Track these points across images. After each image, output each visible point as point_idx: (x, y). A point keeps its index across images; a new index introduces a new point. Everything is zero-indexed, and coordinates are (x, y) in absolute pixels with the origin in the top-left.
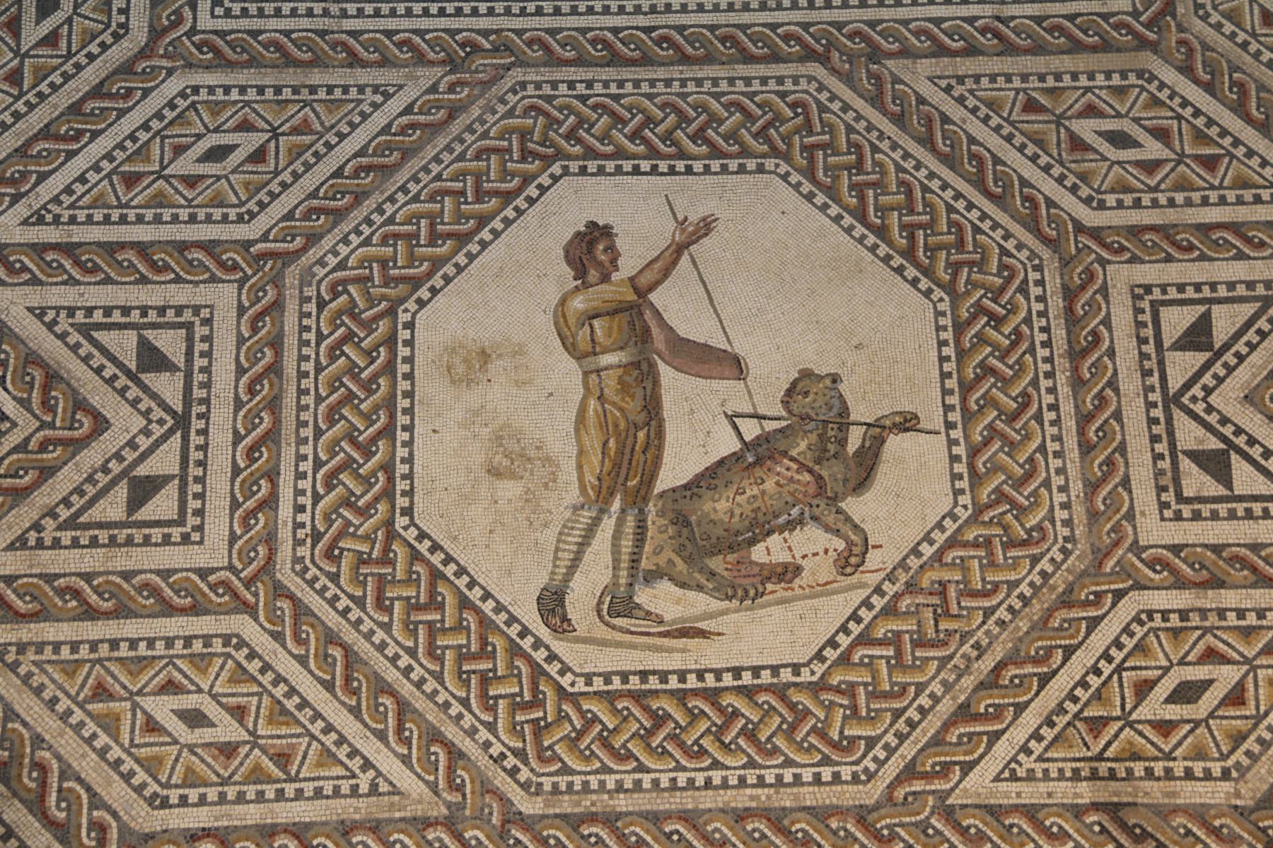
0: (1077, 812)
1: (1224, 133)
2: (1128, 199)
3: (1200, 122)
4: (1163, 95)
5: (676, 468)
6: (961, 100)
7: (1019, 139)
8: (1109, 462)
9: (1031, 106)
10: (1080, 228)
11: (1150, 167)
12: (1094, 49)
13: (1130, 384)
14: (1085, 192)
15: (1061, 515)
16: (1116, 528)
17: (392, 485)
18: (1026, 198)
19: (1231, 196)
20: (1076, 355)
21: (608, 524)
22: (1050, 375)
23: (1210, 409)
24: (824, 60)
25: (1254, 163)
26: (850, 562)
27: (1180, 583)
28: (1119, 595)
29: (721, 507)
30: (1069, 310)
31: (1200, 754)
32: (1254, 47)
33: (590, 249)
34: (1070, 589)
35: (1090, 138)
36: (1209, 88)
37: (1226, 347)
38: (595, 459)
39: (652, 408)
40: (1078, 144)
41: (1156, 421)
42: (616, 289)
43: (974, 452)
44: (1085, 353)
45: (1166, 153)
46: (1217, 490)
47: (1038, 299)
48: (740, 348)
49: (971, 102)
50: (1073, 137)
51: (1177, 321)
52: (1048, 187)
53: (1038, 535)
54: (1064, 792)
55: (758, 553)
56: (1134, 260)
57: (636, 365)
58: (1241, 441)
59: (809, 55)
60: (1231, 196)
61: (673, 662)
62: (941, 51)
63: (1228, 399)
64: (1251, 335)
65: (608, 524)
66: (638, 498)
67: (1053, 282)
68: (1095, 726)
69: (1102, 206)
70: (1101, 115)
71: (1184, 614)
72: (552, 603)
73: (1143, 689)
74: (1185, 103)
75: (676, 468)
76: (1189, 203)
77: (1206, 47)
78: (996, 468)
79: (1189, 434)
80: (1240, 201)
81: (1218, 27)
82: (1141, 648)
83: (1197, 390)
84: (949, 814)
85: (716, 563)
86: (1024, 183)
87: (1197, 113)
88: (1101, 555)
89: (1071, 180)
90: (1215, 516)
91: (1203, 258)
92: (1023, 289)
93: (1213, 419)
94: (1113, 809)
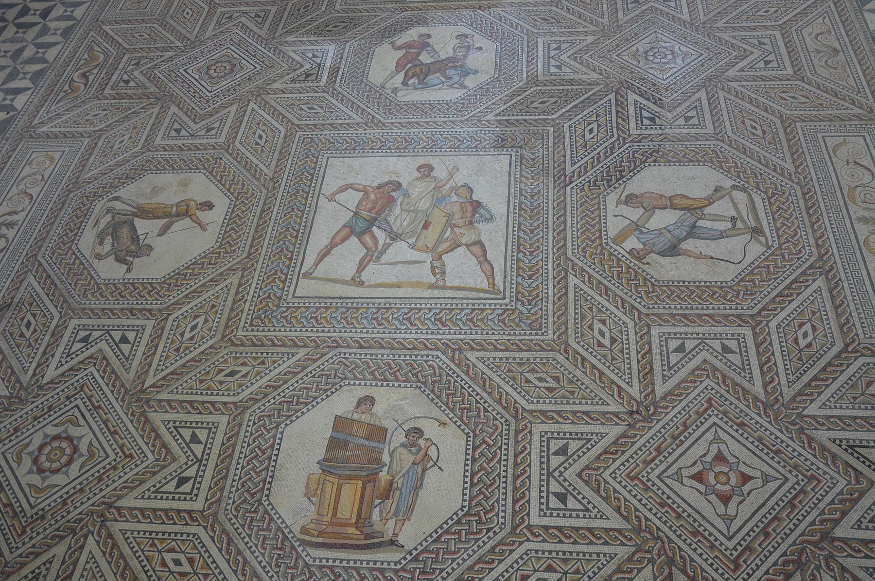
0: (13, 298)
1: (186, 355)
2: (174, 328)
3: (192, 349)
4: (205, 340)
5: (138, 222)
6: (222, 289)
7: (204, 302)
8: (97, 314)
9: (213, 306)
10: (169, 315)
11: (182, 335)
12: (227, 324)
13: (117, 322)
14: (180, 317)
15: (88, 302)
16: (78, 314)
17: (159, 169)
18: (184, 303)
19: (164, 354)
20: (131, 310)
21: (131, 209)
22: (128, 303)
23: (101, 340)
24: (246, 258)
25: (173, 362)
26: (99, 257)
27: (57, 327)
28: (60, 313)
29: (125, 231)
30: (145, 310)
31: (12, 325)
32: (212, 366)
33: (209, 206)
34: (67, 302)
35: (197, 320)
36: (203, 353)
37: (118, 347)
38: (149, 206)
39: (158, 217)
40: (196, 317)
41: (104, 326)
42: (193, 210)
43: (114, 285)
44: (131, 312)
45: (185, 339)
46: (78, 338)
47: (151, 303)
48: (166, 236)
49: (220, 292)
50: (199, 316)
51: (131, 336)
52: (186, 308)
53: (85, 295)
54: (19, 296)
55: (110, 237)
56: (154, 327)
57: (170, 214)
58: (89, 346)
59: (249, 254)
60: (164, 354)
61: (90, 221)
62: (240, 285)
63: (103, 345)
64: (119, 353)
65: (131, 209)
66: (135, 215)
67: (155, 307)
68: (31, 305)
69: (174, 321)
70: (204, 323)
71: (48, 327)
72: (117, 199)
73: (34, 316)
74: (199, 346)
75: (138, 222)
76: (167, 343)
77: (216, 353)
78: (107, 288)
79: (96, 334)
80: (162, 356)
81: (223, 357)
82: (45, 315)
83: (108, 337)
84: (27, 272)
85: (111, 229)
86: (189, 303)
87: (195, 348)
88: (73, 310)
89: (185, 314)
90: (71, 337)
91: (148, 344)
92: (156, 299)
93: (98, 340)
94: (9, 306)
